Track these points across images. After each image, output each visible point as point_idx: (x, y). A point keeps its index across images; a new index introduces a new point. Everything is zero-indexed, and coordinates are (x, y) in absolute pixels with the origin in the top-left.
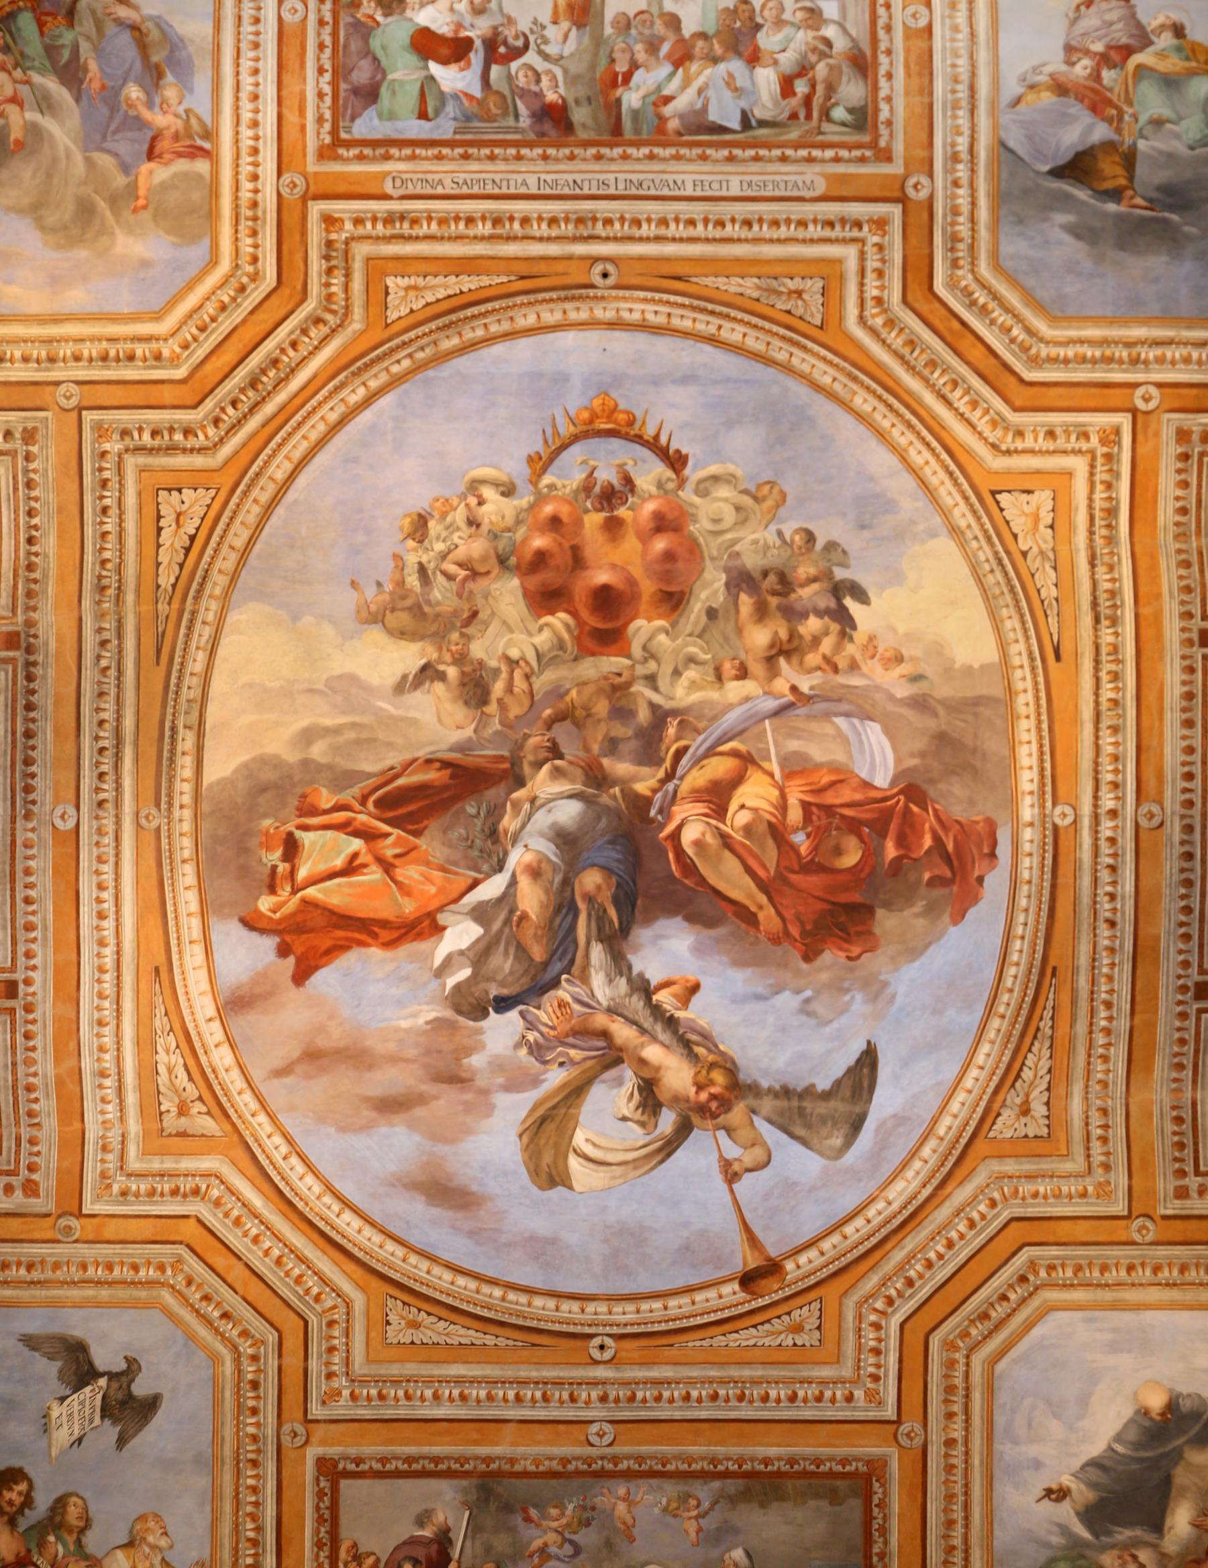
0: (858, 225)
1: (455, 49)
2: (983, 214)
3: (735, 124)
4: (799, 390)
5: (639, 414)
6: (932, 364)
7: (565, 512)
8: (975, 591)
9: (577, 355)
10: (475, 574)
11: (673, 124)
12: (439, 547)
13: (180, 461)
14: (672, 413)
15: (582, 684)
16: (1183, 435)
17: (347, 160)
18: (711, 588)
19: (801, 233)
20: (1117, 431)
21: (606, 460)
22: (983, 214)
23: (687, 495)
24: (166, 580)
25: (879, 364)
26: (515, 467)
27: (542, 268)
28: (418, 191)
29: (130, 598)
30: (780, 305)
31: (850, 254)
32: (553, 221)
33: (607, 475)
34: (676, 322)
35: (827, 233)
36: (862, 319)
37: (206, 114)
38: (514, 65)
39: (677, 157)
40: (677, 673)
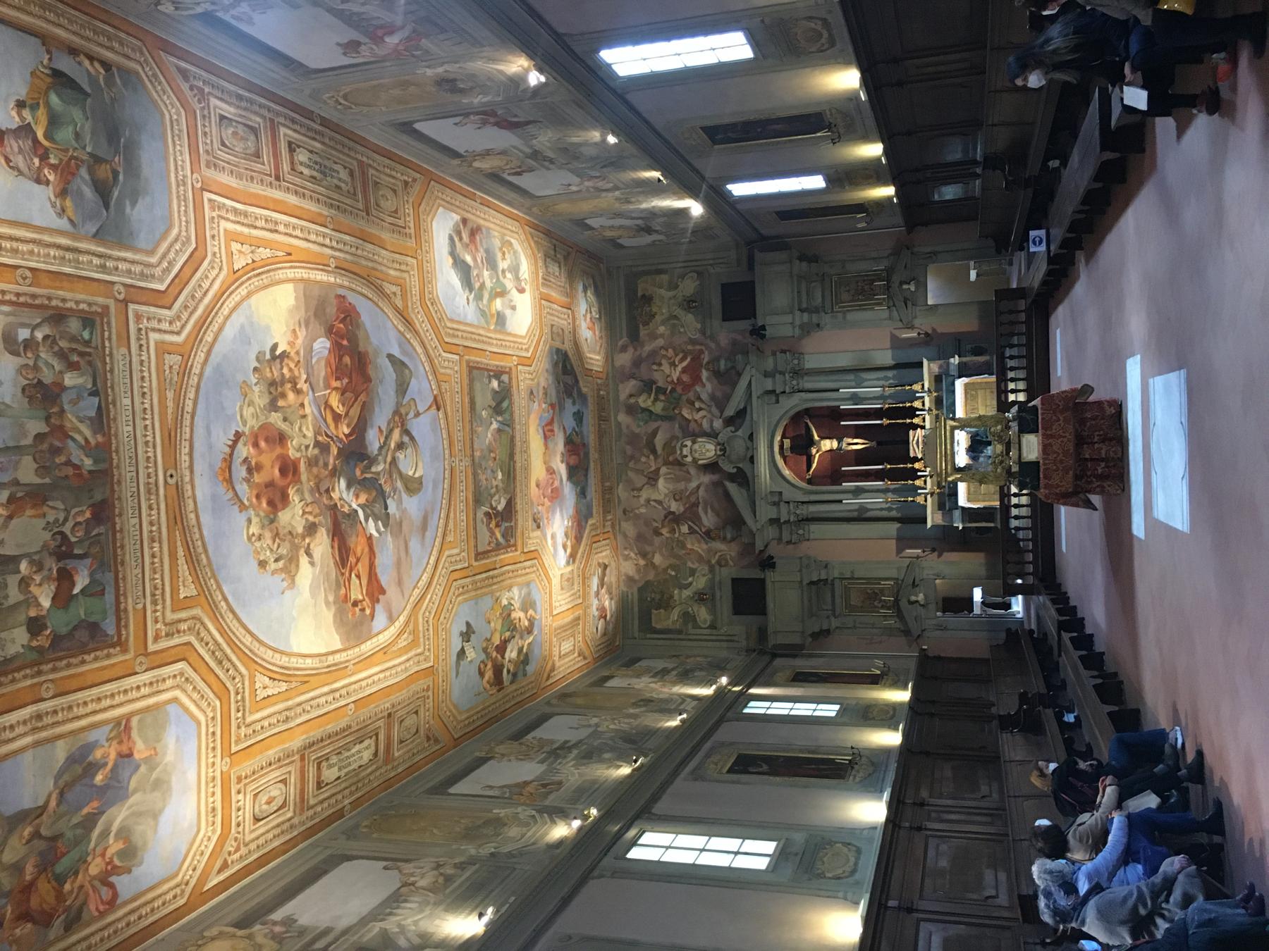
0: (140, 329)
1: (65, 578)
2: (129, 255)
3: (97, 399)
4: (208, 370)
5: (222, 456)
6: (193, 296)
7: (255, 492)
8: (271, 289)
9: (203, 488)
10: (277, 534)
11: (100, 438)
12: (268, 553)
13: (247, 694)
14: (222, 440)
15: (309, 480)
16: (208, 166)
17: (128, 634)
18: (275, 418)
19: (146, 364)
20: (210, 200)
21: (240, 472)
22: (129, 255)
23: (247, 430)
24: (284, 686)
25: (194, 327)
26: (241, 519)
27: (171, 512)
28: (140, 588)
29: (290, 703)
30: (175, 379)
31: (154, 336)
32: (150, 508)
33: (243, 472)
34: (188, 436)
35: (144, 348)
36: (178, 333)
37: (108, 728)
38: (73, 540)
39: (116, 436)
40: (304, 436)
